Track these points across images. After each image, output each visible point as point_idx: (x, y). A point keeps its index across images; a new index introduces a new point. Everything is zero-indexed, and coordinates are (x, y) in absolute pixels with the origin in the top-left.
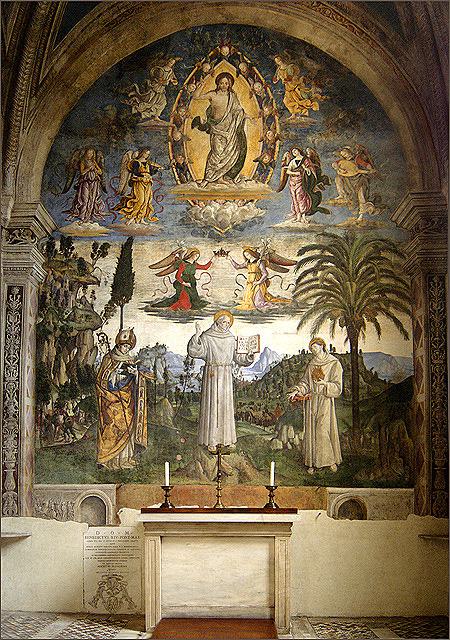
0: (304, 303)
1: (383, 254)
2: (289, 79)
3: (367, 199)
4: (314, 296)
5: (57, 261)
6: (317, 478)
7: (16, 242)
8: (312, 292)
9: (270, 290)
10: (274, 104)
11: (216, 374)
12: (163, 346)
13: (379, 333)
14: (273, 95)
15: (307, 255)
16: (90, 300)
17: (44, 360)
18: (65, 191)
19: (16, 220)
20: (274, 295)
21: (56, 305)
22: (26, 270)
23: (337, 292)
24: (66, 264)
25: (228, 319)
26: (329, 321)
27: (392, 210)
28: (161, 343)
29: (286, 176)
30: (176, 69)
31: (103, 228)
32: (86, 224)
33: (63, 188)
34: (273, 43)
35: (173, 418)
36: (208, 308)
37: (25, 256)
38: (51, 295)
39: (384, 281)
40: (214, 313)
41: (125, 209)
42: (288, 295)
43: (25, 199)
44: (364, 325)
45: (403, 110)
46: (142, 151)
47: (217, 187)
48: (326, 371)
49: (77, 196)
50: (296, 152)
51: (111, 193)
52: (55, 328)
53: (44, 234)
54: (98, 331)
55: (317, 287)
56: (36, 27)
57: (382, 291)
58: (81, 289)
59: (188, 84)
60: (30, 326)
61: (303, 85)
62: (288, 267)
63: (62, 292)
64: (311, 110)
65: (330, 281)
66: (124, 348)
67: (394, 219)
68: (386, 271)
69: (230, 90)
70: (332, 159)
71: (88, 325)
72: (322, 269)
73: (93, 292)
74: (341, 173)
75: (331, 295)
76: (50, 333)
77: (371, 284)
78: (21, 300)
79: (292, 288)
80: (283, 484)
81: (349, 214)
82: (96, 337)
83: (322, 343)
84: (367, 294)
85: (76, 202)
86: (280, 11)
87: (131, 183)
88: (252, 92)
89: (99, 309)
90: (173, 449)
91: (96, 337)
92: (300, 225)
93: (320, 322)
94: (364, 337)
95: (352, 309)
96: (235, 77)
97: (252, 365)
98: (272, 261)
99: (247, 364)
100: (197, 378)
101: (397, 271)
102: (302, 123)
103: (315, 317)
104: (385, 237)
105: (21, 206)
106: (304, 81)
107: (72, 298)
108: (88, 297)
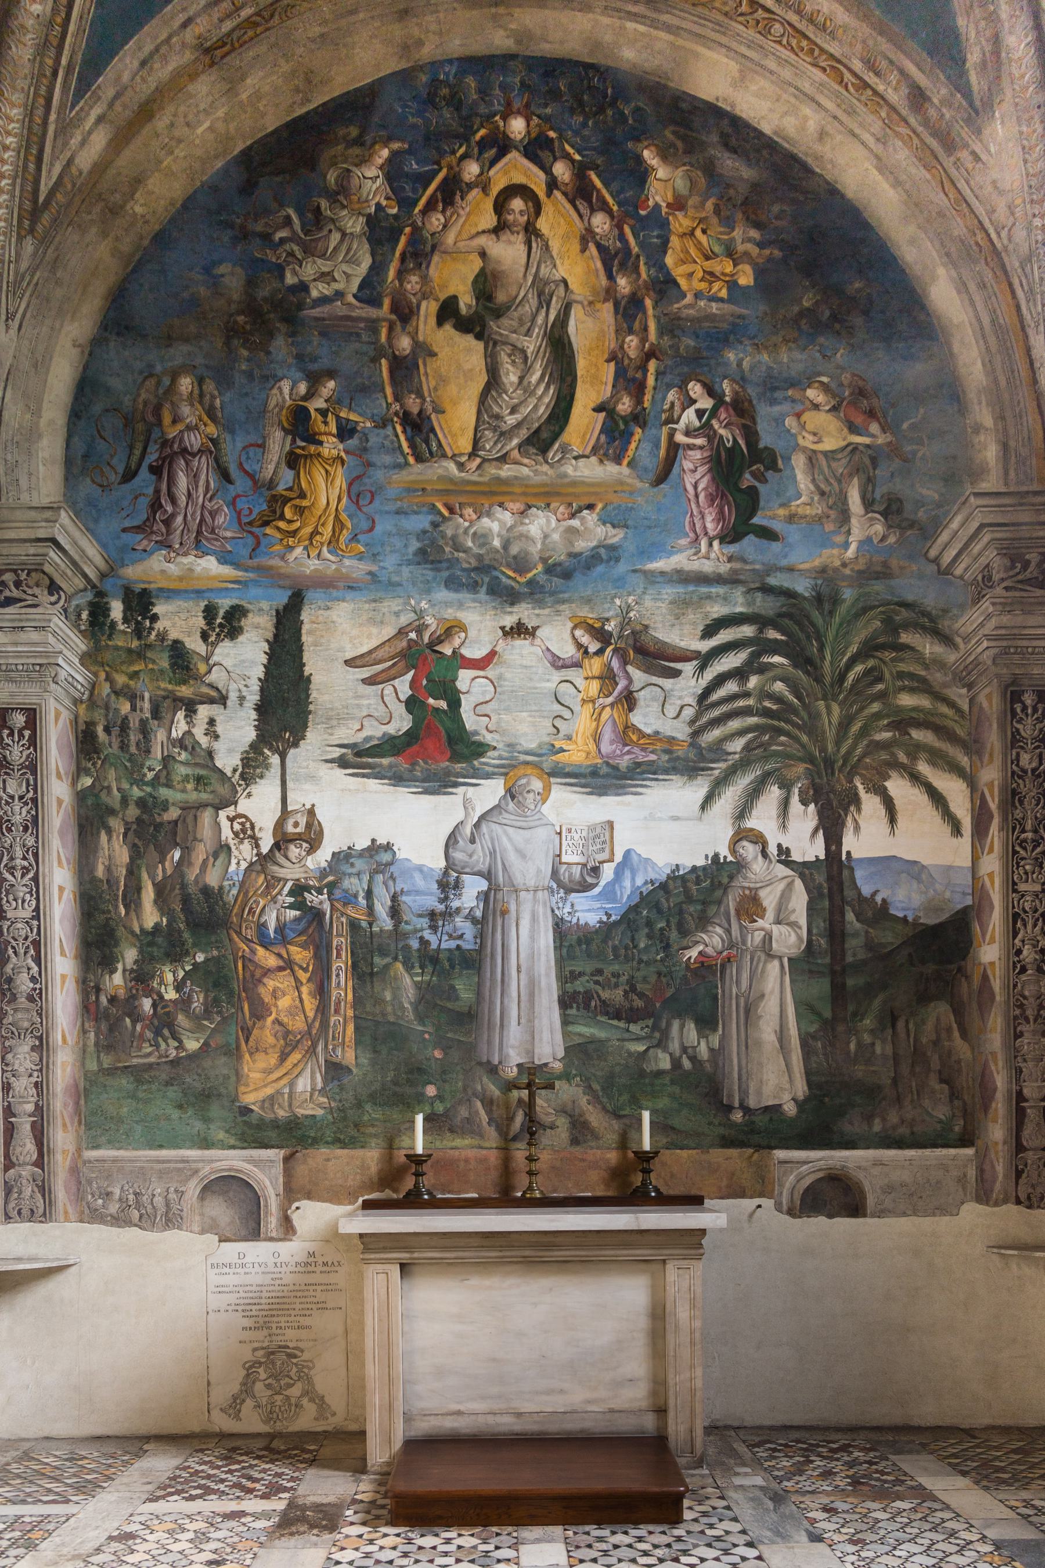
0: (717, 750)
1: (905, 638)
2: (678, 204)
3: (868, 504)
4: (741, 733)
5: (117, 648)
6: (752, 1132)
8: (735, 724)
9: (637, 718)
10: (643, 268)
11: (513, 907)
12: (388, 847)
13: (892, 820)
14: (641, 245)
15: (724, 636)
16: (204, 741)
18: (129, 476)
20: (648, 731)
21: (124, 747)
23: (795, 725)
24: (139, 655)
25: (537, 785)
26: (774, 793)
27: (928, 531)
28: (381, 840)
29: (674, 448)
30: (393, 172)
31: (227, 571)
32: (185, 560)
34: (638, 110)
35: (416, 1009)
36: (490, 759)
37: (34, 636)
38: (107, 730)
39: (906, 700)
40: (507, 770)
41: (282, 524)
42: (680, 731)
44: (856, 801)
45: (962, 287)
46: (315, 380)
47: (506, 471)
48: (769, 899)
49: (157, 491)
50: (695, 389)
51: (241, 484)
52: (125, 801)
53: (79, 583)
54: (230, 811)
55: (746, 712)
57: (903, 722)
58: (180, 715)
59: (425, 212)
61: (715, 220)
62: (678, 666)
63: (134, 723)
64: (732, 285)
65: (778, 699)
66: (294, 851)
67: (933, 553)
68: (912, 676)
69: (531, 231)
70: (786, 407)
71: (204, 796)
72: (762, 669)
73: (212, 722)
74: (807, 441)
75: (780, 731)
77: (876, 707)
79: (689, 713)
80: (672, 1146)
81: (825, 542)
82: (225, 824)
83: (759, 839)
84: (864, 732)
85: (156, 506)
86: (654, 24)
87: (293, 461)
88: (587, 237)
89: (228, 760)
90: (417, 1073)
91: (225, 824)
92: (707, 567)
93: (754, 793)
94: (857, 828)
95: (829, 763)
96: (540, 191)
97: (597, 890)
98: (642, 651)
99: (584, 887)
100: (471, 917)
101: (937, 678)
102: (711, 318)
103: (743, 782)
104: (910, 598)
105: (19, 514)
106: (717, 211)
107: (161, 736)
108: (199, 732)
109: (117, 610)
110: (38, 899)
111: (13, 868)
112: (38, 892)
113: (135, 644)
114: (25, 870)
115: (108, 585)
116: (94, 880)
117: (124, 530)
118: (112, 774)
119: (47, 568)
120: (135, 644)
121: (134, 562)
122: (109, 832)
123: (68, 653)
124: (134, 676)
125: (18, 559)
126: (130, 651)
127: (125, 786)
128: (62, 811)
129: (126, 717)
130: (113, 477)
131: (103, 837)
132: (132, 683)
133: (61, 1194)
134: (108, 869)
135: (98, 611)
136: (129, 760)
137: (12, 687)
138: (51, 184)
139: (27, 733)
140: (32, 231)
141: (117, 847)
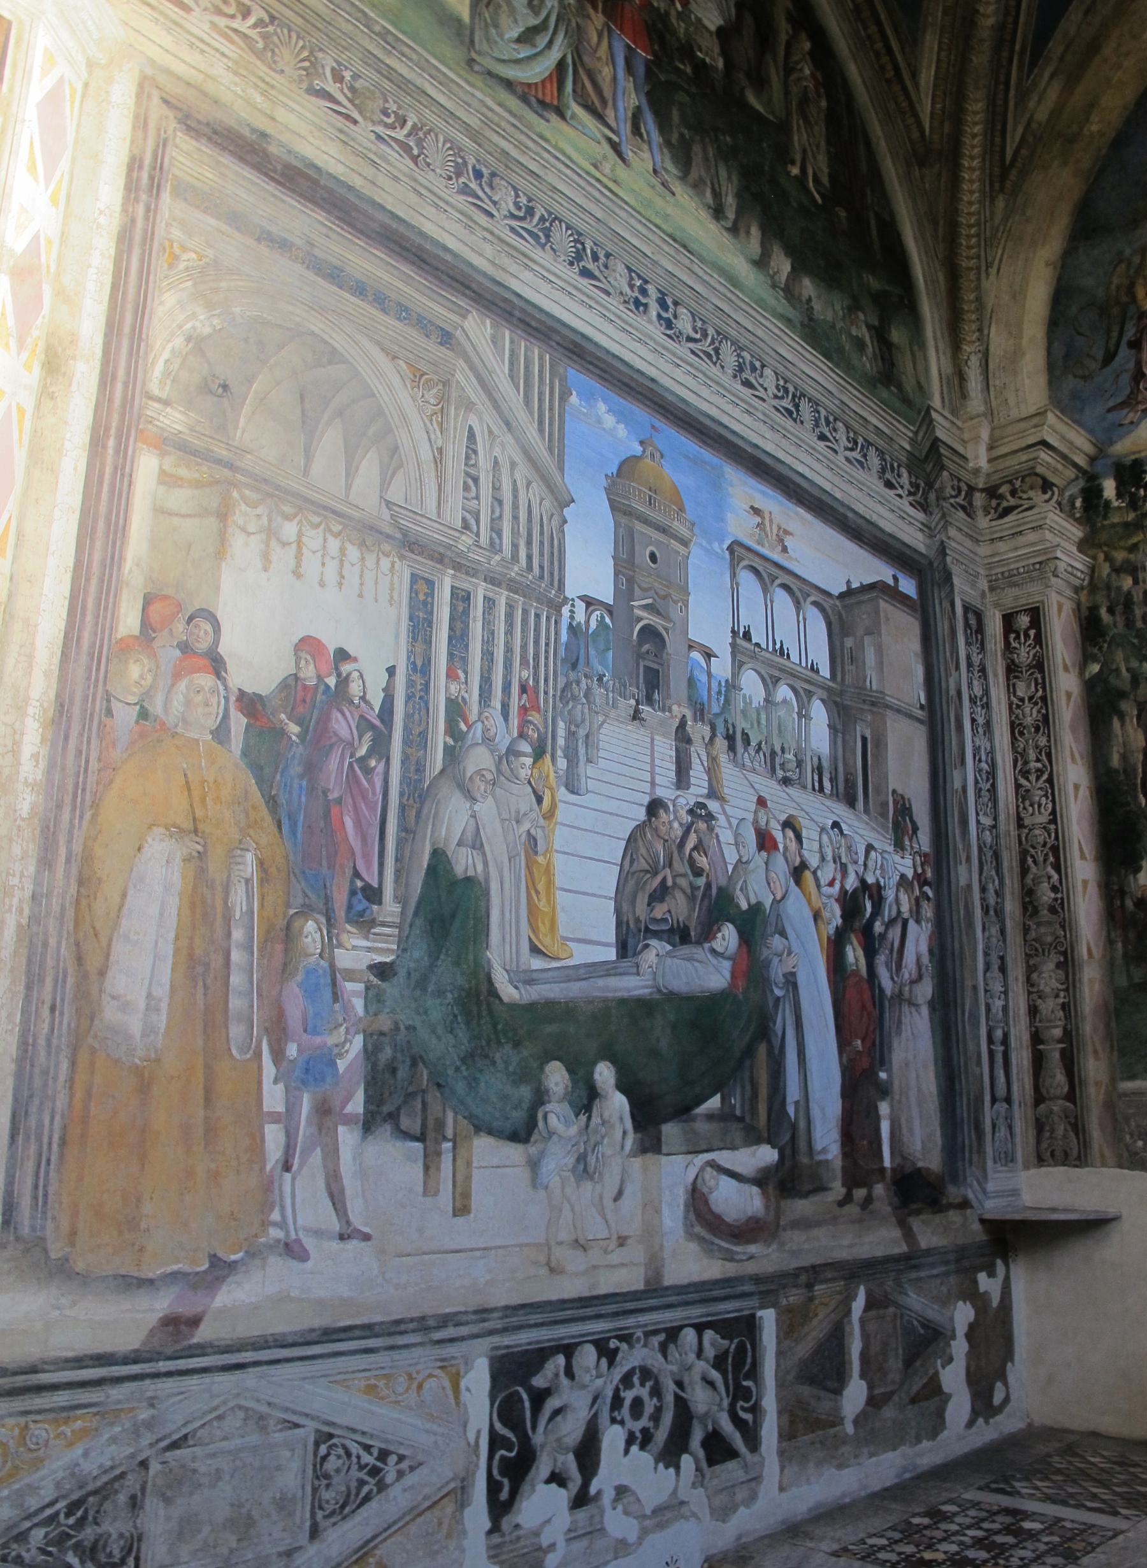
5: (1113, 526)
7: (1007, 511)
17: (1115, 761)
18: (1109, 358)
19: (1001, 464)
21: (1129, 624)
22: (1043, 567)
33: (1100, 355)
37: (1032, 537)
38: (1111, 611)
43: (1015, 414)
53: (1071, 473)
56: (980, 59)
60: (1069, 695)
76: (1123, 695)
78: (1038, 639)
105: (1009, 430)
109: (1109, 488)
110: (1053, 801)
111: (1028, 772)
112: (1053, 794)
113: (1131, 516)
114: (1040, 772)
115: (1099, 467)
116: (1110, 772)
117: (1109, 410)
118: (1119, 655)
119: (1039, 470)
120: (1131, 516)
121: (1121, 437)
122: (1122, 717)
123: (1063, 544)
124: (1134, 548)
125: (1011, 470)
126: (1126, 525)
127: (1135, 664)
128: (1072, 704)
129: (1129, 593)
130: (1094, 366)
131: (1116, 723)
132: (1132, 556)
133: (1096, 1134)
134: (1124, 757)
135: (1092, 494)
136: (1137, 637)
137: (1013, 592)
138: (1015, 145)
139: (1032, 633)
140: (1002, 190)
141: (1131, 731)
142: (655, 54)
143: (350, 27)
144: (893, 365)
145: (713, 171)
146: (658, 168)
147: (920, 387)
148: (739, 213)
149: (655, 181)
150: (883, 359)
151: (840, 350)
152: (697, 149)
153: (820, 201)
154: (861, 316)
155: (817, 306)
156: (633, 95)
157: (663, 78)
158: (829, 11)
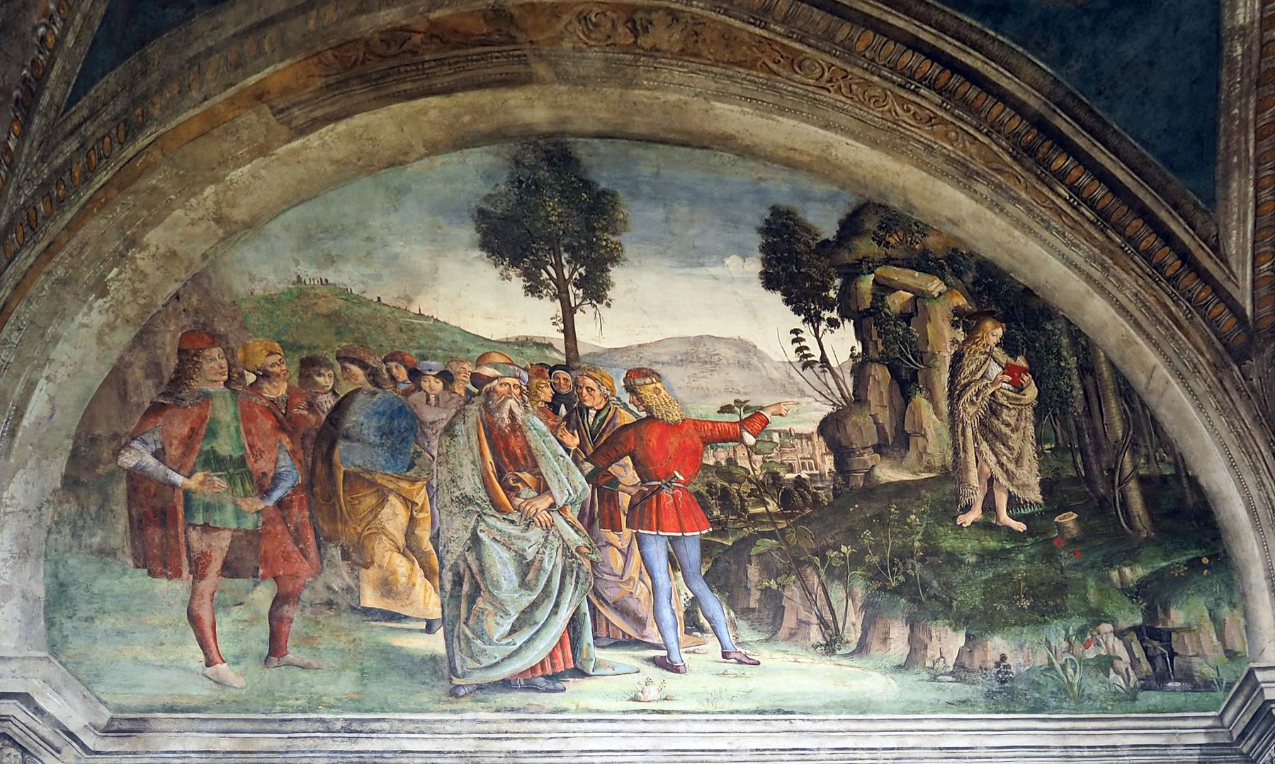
142: (717, 522)
143: (310, 742)
144: (1173, 655)
145: (821, 602)
146: (730, 648)
147: (1232, 655)
148: (872, 616)
149: (731, 667)
150: (1151, 659)
151: (1064, 690)
152: (793, 593)
153: (1020, 527)
154: (1106, 627)
155: (1016, 662)
156: (684, 589)
157: (730, 544)
158: (1034, 249)
